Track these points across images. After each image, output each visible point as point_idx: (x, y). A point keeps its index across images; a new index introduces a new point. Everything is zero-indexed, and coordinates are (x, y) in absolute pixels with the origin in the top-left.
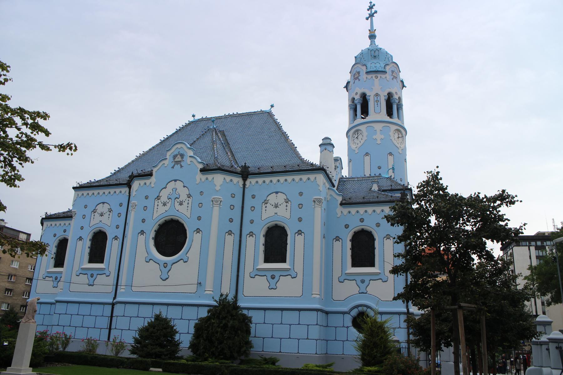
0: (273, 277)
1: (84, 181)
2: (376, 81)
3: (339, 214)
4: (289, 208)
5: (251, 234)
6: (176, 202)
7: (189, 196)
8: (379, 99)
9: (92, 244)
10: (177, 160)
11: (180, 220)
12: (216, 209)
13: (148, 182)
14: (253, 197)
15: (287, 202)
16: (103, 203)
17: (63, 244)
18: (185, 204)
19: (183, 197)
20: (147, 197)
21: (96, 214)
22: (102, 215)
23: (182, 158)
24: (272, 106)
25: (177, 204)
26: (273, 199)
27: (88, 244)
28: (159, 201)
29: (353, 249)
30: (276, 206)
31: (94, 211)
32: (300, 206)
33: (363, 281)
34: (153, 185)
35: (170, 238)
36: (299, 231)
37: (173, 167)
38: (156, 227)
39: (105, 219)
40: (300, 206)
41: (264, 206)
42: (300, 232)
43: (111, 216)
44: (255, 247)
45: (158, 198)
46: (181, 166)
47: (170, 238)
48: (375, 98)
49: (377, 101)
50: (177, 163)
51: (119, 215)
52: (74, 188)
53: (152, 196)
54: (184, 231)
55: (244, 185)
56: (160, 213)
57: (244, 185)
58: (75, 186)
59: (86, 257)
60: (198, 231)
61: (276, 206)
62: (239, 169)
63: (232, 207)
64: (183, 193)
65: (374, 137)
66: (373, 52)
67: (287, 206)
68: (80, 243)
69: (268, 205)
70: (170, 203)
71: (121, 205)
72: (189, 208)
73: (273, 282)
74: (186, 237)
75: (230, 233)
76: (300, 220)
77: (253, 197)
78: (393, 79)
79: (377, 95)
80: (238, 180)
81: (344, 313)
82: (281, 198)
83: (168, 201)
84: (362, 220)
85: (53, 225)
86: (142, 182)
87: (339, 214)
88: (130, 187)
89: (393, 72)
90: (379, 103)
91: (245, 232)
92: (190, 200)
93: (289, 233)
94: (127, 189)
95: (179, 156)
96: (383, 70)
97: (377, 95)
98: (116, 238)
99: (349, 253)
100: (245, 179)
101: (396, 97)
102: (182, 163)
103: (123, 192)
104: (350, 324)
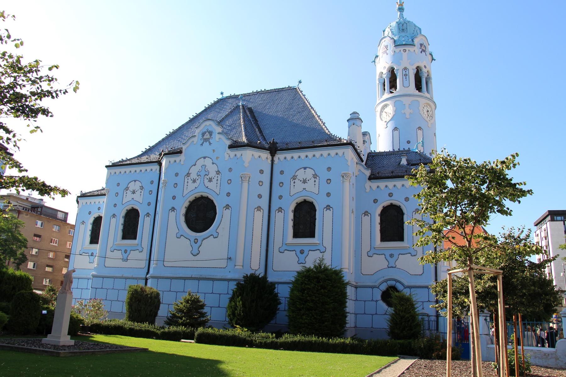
0: (302, 252)
1: (117, 160)
2: (405, 55)
3: (368, 189)
4: (317, 183)
5: (280, 210)
6: (205, 179)
7: (218, 172)
8: (407, 73)
9: (125, 221)
11: (210, 197)
12: (245, 185)
13: (177, 158)
14: (282, 172)
15: (315, 178)
16: (135, 181)
17: (97, 222)
18: (214, 181)
19: (212, 174)
20: (177, 175)
21: (128, 191)
22: (134, 192)
23: (211, 135)
24: (300, 82)
25: (206, 181)
26: (301, 174)
27: (122, 221)
28: (189, 178)
29: (381, 223)
31: (127, 189)
32: (329, 181)
33: (391, 256)
34: (182, 163)
35: (201, 214)
36: (327, 206)
37: (202, 145)
38: (187, 204)
39: (137, 196)
40: (329, 181)
41: (292, 182)
42: (328, 207)
43: (142, 194)
45: (188, 175)
46: (210, 144)
47: (201, 214)
48: (404, 72)
49: (406, 75)
50: (206, 140)
51: (151, 192)
52: (107, 167)
53: (183, 173)
54: (214, 207)
55: (273, 161)
56: (191, 191)
57: (273, 161)
58: (108, 164)
59: (120, 234)
60: (227, 207)
61: (305, 181)
62: (267, 146)
63: (261, 183)
64: (212, 170)
65: (403, 112)
66: (401, 25)
67: (315, 181)
68: (114, 220)
69: (296, 181)
70: (199, 180)
71: (152, 182)
72: (219, 185)
73: (302, 257)
74: (216, 214)
75: (259, 208)
76: (328, 195)
78: (421, 52)
79: (405, 69)
80: (265, 155)
81: (372, 287)
83: (197, 178)
84: (391, 195)
85: (88, 203)
86: (172, 159)
87: (368, 189)
88: (160, 164)
89: (421, 45)
90: (407, 77)
92: (219, 176)
93: (317, 208)
94: (158, 167)
95: (207, 133)
96: (411, 43)
97: (405, 69)
98: (148, 215)
99: (378, 227)
100: (273, 154)
101: (424, 70)
102: (211, 141)
103: (154, 170)
104: (379, 298)
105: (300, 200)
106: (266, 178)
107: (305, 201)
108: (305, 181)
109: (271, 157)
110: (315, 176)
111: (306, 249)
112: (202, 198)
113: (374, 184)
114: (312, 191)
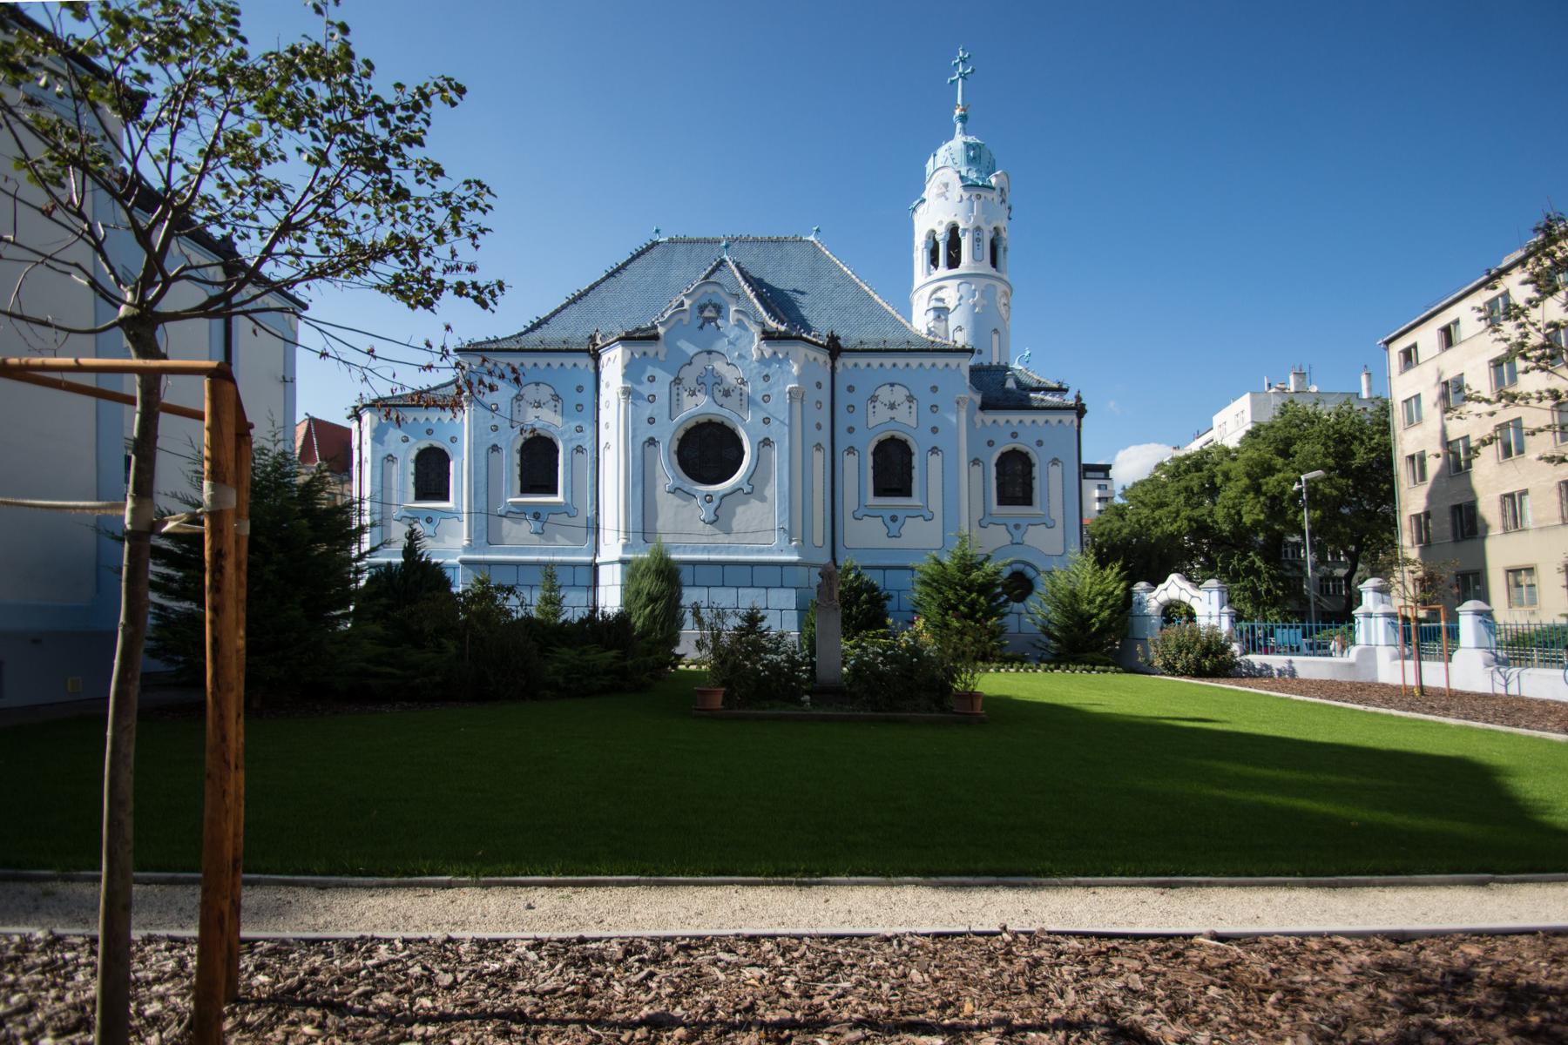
3: (979, 425)
5: (851, 450)
10: (707, 314)
13: (651, 349)
14: (851, 389)
18: (736, 395)
25: (718, 396)
26: (885, 394)
30: (892, 406)
32: (934, 408)
34: (661, 357)
35: (708, 452)
37: (701, 327)
38: (681, 434)
40: (934, 408)
41: (870, 409)
42: (934, 450)
44: (858, 472)
47: (708, 452)
55: (833, 368)
57: (833, 368)
75: (819, 447)
77: (851, 389)
80: (823, 357)
82: (899, 394)
86: (638, 350)
87: (979, 425)
91: (841, 447)
102: (719, 322)
105: (883, 436)
106: (824, 396)
107: (893, 439)
108: (892, 406)
109: (829, 361)
110: (910, 399)
111: (900, 515)
112: (710, 423)
113: (989, 417)
114: (905, 421)
